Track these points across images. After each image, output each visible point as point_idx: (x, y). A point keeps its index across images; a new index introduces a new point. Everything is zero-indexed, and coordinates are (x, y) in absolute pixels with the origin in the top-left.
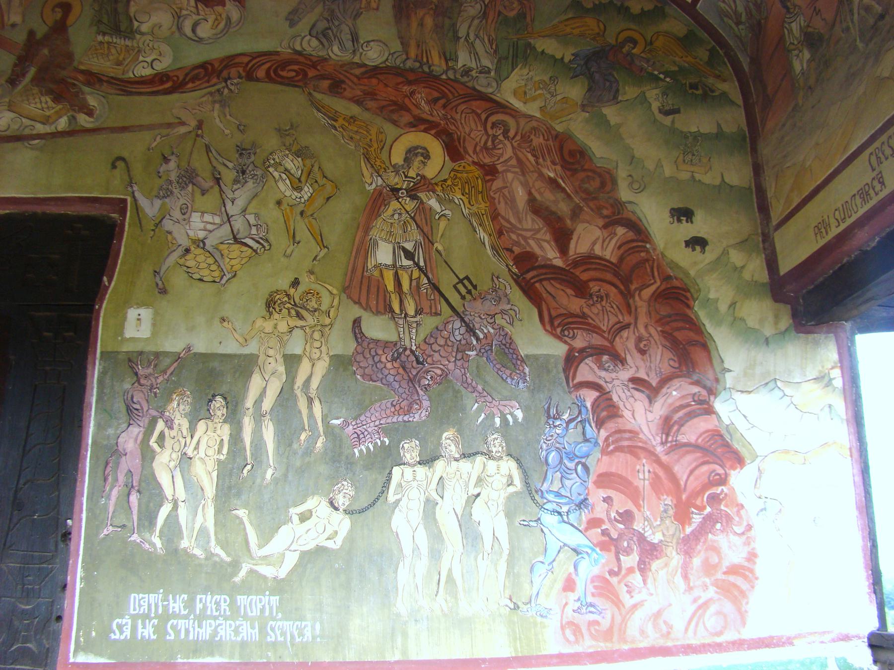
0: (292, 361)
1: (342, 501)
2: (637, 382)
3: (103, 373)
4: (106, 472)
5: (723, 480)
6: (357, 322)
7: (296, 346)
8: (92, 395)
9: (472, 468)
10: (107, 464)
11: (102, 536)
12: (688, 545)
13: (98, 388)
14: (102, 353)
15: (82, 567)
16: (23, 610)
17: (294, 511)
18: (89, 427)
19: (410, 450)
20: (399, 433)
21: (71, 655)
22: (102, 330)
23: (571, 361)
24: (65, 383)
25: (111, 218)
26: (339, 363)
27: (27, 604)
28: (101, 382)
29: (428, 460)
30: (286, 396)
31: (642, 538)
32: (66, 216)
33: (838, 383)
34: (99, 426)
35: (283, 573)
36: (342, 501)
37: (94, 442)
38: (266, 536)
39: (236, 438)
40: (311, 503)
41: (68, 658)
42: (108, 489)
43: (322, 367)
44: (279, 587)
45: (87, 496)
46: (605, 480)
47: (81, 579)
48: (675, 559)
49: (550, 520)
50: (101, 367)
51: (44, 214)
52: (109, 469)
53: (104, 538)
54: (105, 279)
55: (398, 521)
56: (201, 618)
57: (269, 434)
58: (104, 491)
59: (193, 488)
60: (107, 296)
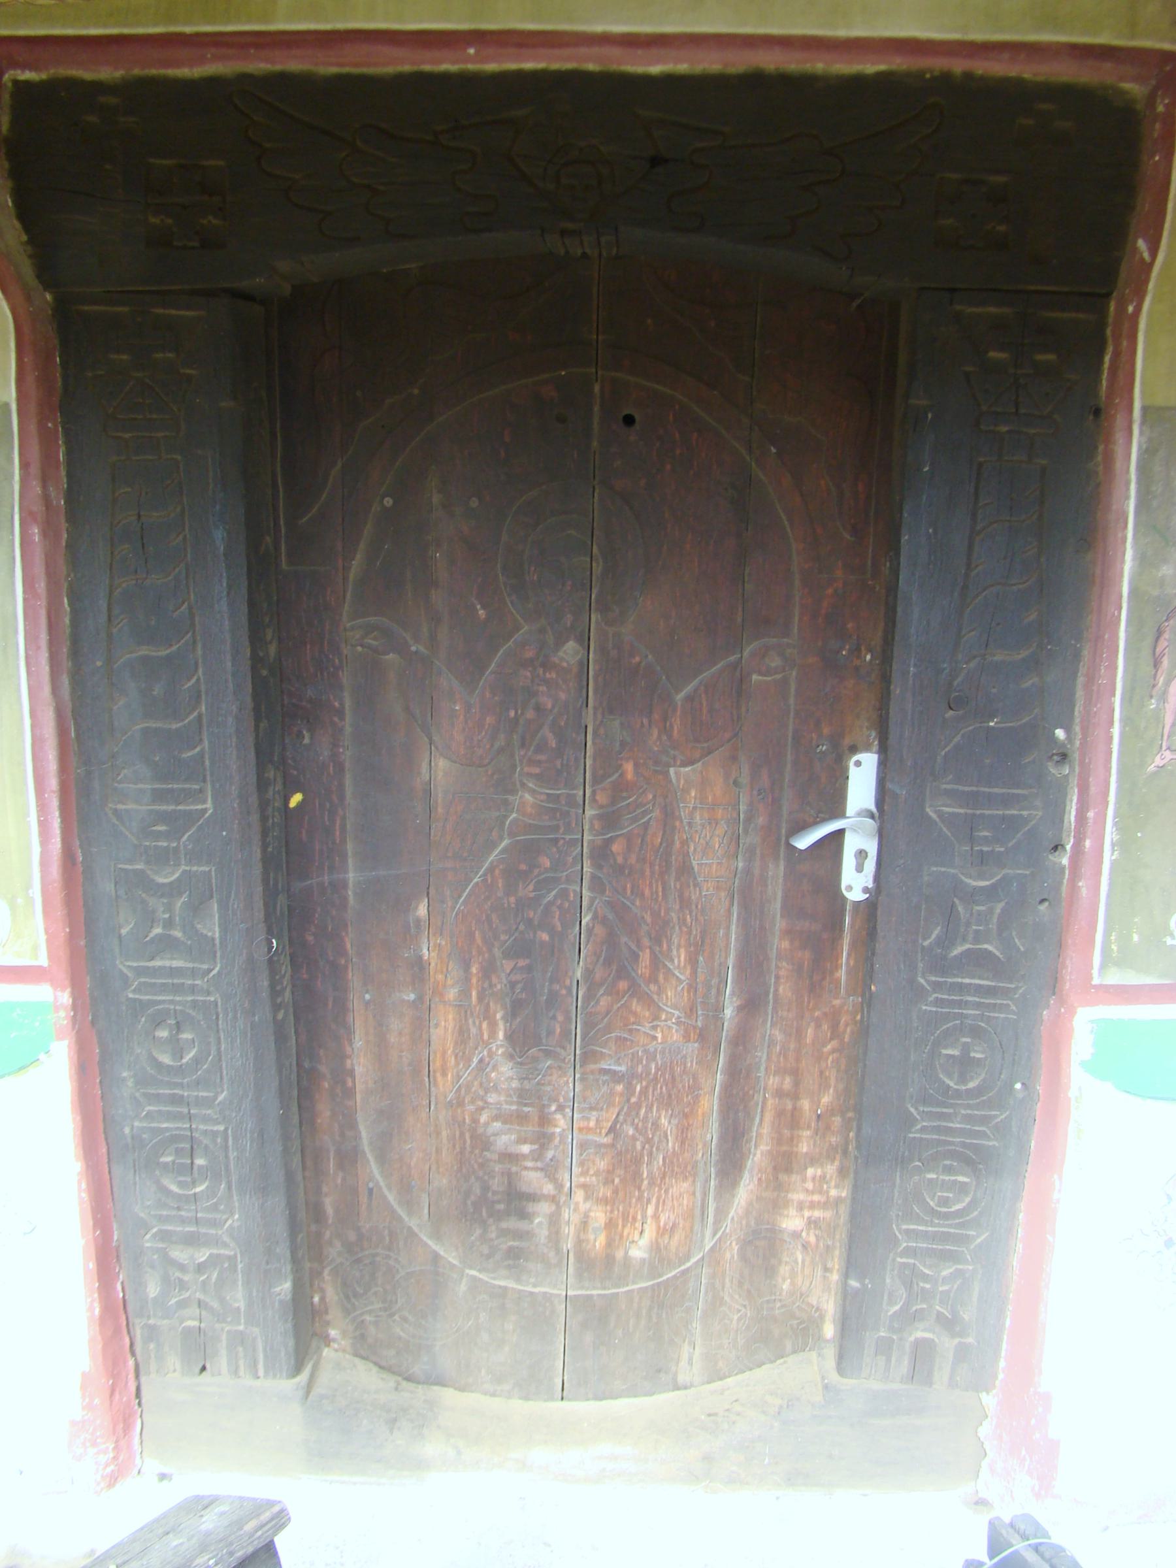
3: (1148, 453)
4: (1158, 650)
8: (1127, 498)
10: (1159, 633)
11: (1151, 768)
13: (1139, 482)
14: (1145, 409)
15: (1115, 824)
16: (975, 888)
18: (1123, 562)
21: (1095, 972)
22: (1144, 360)
24: (1044, 462)
25: (1123, 93)
27: (981, 876)
28: (1143, 469)
32: (1019, 83)
34: (1143, 560)
37: (1133, 592)
41: (1091, 978)
42: (1161, 680)
45: (1123, 694)
47: (1113, 845)
50: (1144, 439)
51: (968, 76)
52: (1163, 644)
53: (1155, 773)
54: (1141, 244)
58: (1154, 686)
60: (1151, 286)
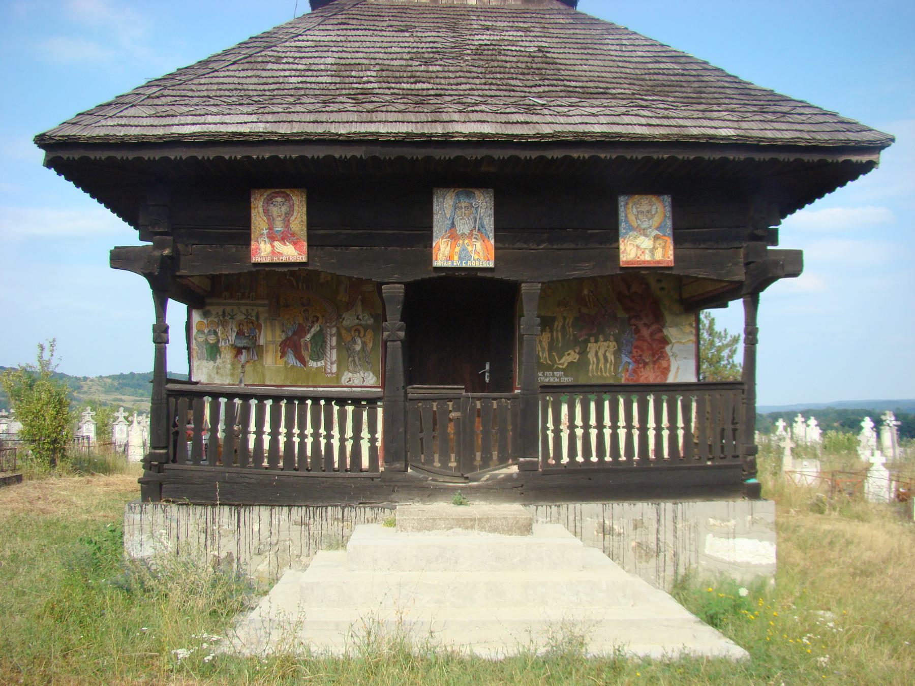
0: (564, 318)
1: (577, 351)
2: (645, 325)
5: (663, 348)
6: (580, 309)
7: (565, 315)
9: (606, 344)
12: (655, 363)
17: (566, 353)
19: (592, 339)
20: (589, 335)
23: (630, 319)
26: (576, 319)
29: (596, 342)
30: (563, 327)
31: (643, 360)
33: (694, 325)
35: (564, 367)
36: (577, 351)
38: (560, 359)
39: (552, 336)
40: (570, 351)
43: (572, 320)
44: (563, 370)
46: (637, 347)
48: (651, 365)
49: (623, 356)
55: (590, 356)
56: (546, 377)
57: (560, 335)
59: (543, 349)
